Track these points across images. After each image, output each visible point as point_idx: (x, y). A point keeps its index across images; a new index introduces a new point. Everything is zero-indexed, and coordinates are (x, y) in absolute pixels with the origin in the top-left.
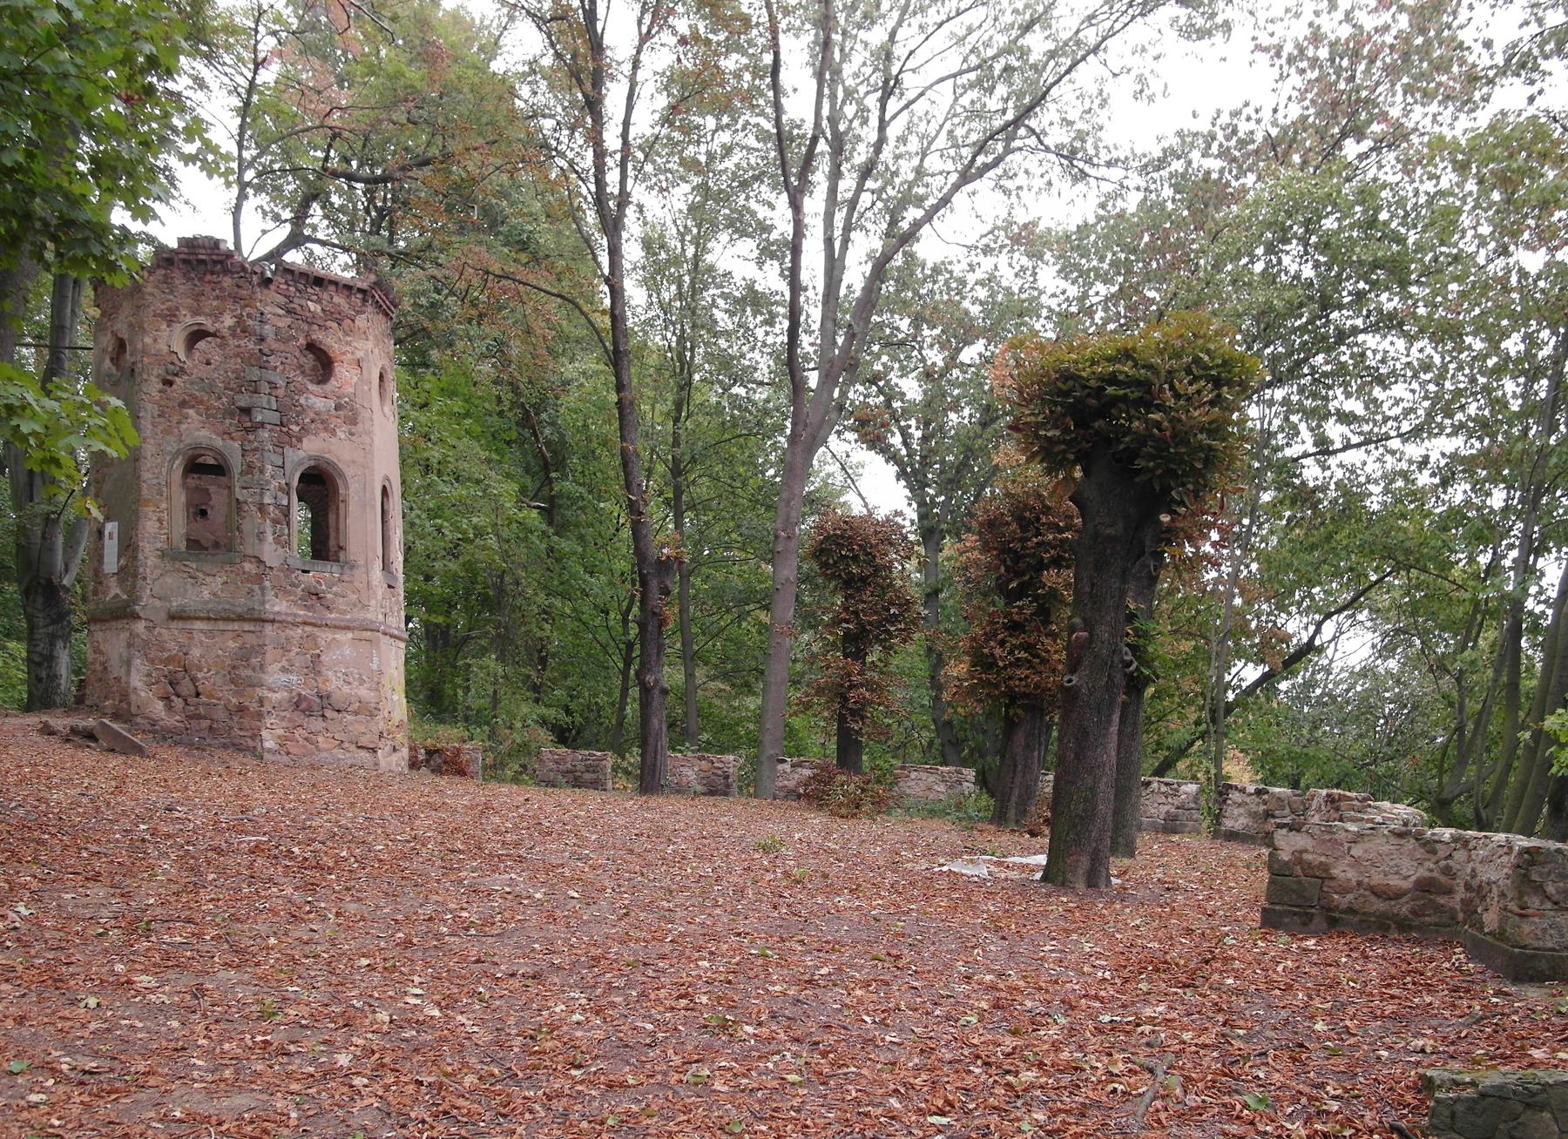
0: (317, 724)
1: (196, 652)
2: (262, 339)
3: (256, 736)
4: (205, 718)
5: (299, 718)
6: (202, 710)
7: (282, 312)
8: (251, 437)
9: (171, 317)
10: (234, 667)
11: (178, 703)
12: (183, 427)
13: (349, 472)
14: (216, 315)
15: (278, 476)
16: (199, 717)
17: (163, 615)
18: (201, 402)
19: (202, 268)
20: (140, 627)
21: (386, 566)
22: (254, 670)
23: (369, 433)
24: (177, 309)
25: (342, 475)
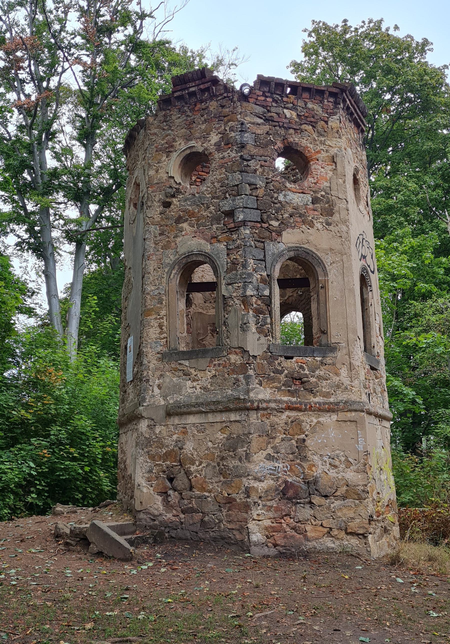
0: (305, 512)
1: (189, 447)
2: (243, 146)
3: (244, 529)
4: (196, 511)
5: (285, 507)
6: (194, 504)
8: (235, 237)
10: (223, 459)
11: (173, 496)
12: (179, 240)
13: (327, 259)
14: (205, 137)
15: (261, 274)
16: (192, 511)
17: (162, 413)
18: (192, 214)
19: (194, 100)
20: (143, 425)
21: (368, 348)
22: (240, 460)
23: (345, 222)
24: (174, 140)
25: (321, 263)
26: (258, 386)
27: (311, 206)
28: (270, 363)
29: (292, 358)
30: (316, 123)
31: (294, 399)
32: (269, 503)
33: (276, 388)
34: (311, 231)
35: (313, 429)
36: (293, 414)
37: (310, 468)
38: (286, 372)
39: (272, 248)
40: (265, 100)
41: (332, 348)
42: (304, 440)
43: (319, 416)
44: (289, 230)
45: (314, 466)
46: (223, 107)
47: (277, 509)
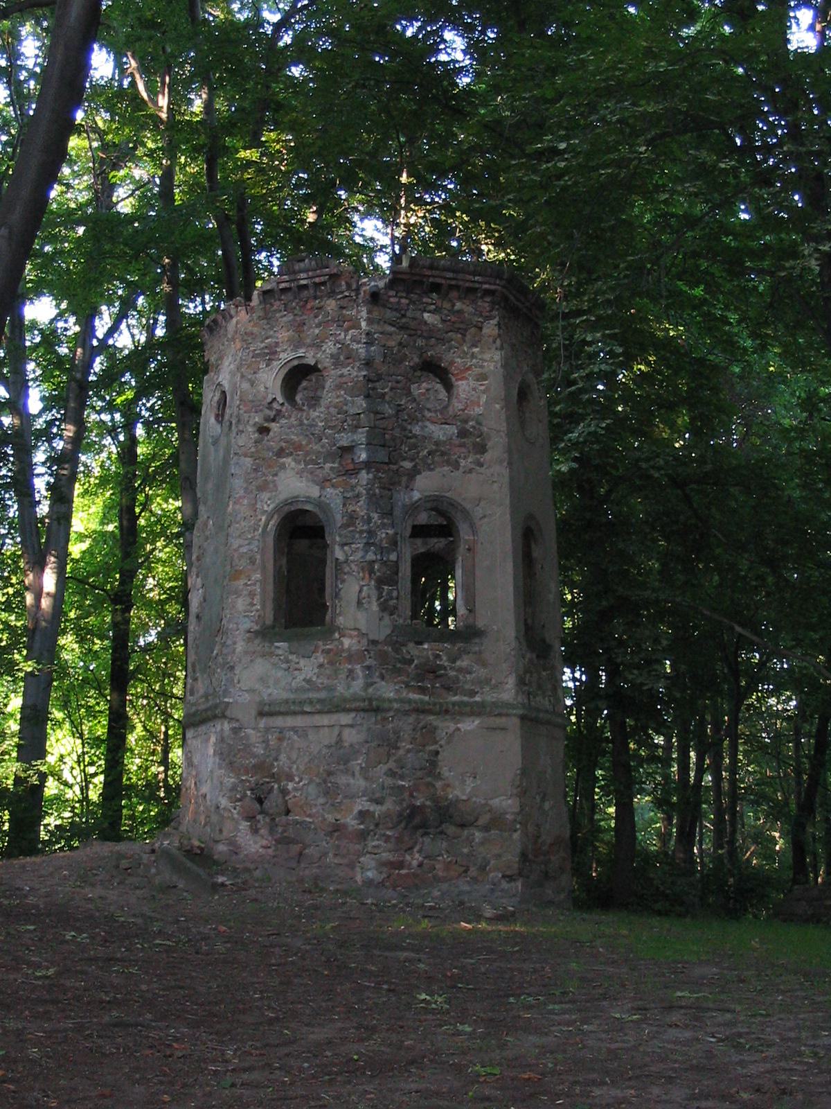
6: (290, 833)
8: (354, 481)
9: (270, 354)
10: (330, 774)
14: (317, 345)
18: (299, 447)
26: (378, 680)
27: (457, 442)
28: (397, 651)
30: (466, 330)
31: (427, 698)
32: (388, 833)
33: (403, 682)
34: (457, 474)
35: (451, 737)
40: (399, 303)
42: (437, 753)
43: (458, 722)
44: (426, 474)
45: (448, 786)
46: (342, 308)
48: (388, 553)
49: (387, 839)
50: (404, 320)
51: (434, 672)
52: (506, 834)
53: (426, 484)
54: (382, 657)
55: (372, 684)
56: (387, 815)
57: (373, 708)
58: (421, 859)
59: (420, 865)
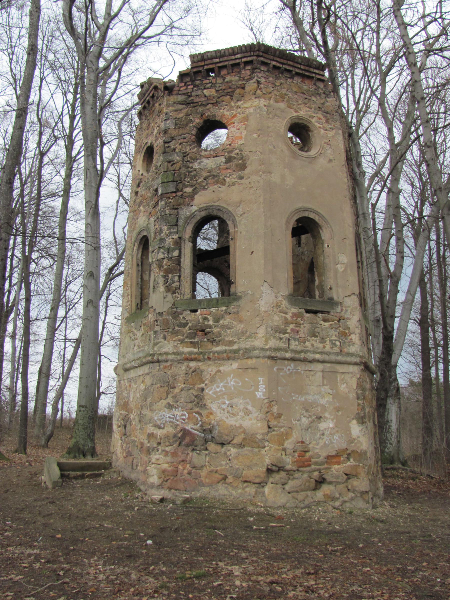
7: (181, 107)
26: (162, 340)
29: (196, 311)
30: (233, 92)
32: (168, 449)
34: (223, 188)
36: (193, 364)
37: (208, 416)
38: (190, 324)
39: (185, 212)
41: (237, 298)
42: (203, 390)
43: (220, 365)
45: (211, 414)
47: (174, 454)
48: (173, 252)
49: (166, 453)
50: (190, 99)
51: (203, 331)
52: (256, 450)
53: (201, 201)
54: (166, 323)
55: (158, 343)
56: (167, 437)
57: (154, 360)
58: (190, 469)
59: (189, 473)
